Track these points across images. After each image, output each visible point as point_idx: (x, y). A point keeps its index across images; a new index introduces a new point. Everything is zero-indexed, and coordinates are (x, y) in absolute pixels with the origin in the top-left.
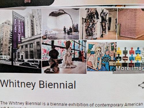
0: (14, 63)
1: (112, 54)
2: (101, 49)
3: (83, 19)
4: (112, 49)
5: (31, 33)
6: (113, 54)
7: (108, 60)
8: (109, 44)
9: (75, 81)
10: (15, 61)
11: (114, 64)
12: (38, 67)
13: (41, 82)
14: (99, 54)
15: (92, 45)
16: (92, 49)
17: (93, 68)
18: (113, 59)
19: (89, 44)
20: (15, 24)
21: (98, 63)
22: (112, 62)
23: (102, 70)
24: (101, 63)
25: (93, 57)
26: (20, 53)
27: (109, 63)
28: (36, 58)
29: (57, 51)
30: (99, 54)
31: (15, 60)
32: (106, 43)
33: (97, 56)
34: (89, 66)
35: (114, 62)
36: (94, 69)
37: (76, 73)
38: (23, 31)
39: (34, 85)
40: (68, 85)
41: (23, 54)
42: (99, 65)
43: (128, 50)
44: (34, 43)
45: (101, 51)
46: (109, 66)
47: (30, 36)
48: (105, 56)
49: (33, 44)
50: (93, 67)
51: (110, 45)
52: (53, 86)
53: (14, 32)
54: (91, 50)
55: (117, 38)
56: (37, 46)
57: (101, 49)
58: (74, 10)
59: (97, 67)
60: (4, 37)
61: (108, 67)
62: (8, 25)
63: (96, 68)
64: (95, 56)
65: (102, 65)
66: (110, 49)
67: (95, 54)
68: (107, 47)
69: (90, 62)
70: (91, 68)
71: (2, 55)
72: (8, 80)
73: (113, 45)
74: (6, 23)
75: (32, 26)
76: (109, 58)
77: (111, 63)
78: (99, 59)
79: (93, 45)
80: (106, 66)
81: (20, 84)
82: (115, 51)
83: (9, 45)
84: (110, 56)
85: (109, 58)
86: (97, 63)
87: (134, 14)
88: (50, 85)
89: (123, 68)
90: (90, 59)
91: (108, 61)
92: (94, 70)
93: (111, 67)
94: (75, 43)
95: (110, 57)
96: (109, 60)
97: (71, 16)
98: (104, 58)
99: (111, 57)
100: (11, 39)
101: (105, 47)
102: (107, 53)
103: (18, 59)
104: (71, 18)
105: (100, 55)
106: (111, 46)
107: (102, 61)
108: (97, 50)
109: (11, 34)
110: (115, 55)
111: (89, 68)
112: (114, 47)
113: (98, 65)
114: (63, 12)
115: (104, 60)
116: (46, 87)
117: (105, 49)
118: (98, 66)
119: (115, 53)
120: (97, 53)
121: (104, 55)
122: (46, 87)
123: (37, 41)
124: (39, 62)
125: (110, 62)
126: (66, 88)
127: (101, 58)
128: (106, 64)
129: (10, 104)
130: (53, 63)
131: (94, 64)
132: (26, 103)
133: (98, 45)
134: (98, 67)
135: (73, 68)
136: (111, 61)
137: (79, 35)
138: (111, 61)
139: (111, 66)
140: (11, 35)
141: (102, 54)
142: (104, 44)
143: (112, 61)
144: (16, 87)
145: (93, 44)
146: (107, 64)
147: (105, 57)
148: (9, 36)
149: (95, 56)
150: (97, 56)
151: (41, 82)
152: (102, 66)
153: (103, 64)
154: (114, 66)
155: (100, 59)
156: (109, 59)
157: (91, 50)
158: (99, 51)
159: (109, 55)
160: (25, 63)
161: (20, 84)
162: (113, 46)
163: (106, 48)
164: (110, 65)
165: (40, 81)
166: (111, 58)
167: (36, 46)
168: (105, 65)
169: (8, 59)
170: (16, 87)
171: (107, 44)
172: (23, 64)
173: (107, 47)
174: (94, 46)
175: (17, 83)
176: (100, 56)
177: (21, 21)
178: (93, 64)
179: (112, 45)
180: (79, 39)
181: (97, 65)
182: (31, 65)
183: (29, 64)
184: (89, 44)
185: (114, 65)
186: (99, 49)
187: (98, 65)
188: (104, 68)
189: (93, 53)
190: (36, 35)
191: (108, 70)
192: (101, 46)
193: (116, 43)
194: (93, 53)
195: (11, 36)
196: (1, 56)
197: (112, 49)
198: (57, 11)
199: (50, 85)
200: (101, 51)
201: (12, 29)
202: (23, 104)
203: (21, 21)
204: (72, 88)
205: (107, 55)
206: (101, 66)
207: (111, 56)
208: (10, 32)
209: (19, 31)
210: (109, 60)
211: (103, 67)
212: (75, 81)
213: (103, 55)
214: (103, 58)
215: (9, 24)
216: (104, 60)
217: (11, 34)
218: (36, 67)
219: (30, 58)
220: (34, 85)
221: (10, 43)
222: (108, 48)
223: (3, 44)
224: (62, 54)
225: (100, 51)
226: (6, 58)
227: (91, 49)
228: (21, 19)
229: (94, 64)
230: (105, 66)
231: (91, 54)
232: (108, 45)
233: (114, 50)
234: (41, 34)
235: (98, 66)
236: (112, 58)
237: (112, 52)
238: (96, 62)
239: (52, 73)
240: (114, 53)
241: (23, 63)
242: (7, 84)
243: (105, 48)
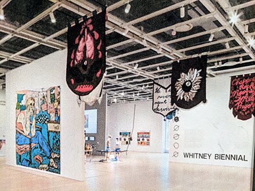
2: (34, 100)
4: (53, 101)
7: (46, 120)
8: (47, 91)
16: (22, 101)
19: (18, 95)
21: (31, 124)
22: (52, 124)
24: (36, 125)
32: (41, 91)
34: (18, 130)
35: (56, 125)
36: (25, 135)
42: (32, 129)
46: (48, 133)
48: (41, 113)
51: (49, 92)
54: (20, 104)
57: (34, 100)
59: (29, 132)
63: (28, 135)
66: (49, 101)
67: (26, 111)
68: (44, 97)
69: (19, 123)
76: (46, 117)
77: (51, 127)
79: (24, 95)
82: (57, 104)
84: (49, 113)
85: (46, 117)
86: (29, 125)
90: (20, 119)
93: (50, 133)
95: (49, 114)
96: (48, 120)
98: (39, 117)
99: (51, 114)
101: (41, 97)
105: (34, 112)
107: (37, 122)
108: (29, 104)
110: (57, 112)
111: (20, 133)
112: (55, 97)
113: (31, 128)
115: (39, 120)
119: (58, 108)
120: (28, 108)
121: (40, 112)
125: (48, 124)
127: (35, 116)
131: (26, 127)
133: (29, 95)
134: (30, 132)
136: (51, 122)
139: (52, 131)
142: (39, 92)
143: (53, 122)
145: (24, 93)
150: (27, 113)
153: (38, 128)
155: (34, 119)
156: (47, 119)
157: (20, 104)
158: (31, 104)
159: (47, 111)
162: (54, 94)
163: (43, 99)
164: (49, 129)
166: (50, 116)
173: (44, 97)
174: (24, 97)
176: (32, 113)
178: (24, 126)
179: (52, 93)
181: (29, 129)
184: (18, 95)
186: (32, 102)
187: (31, 128)
192: (34, 96)
193: (59, 87)
197: (51, 99)
200: (34, 104)
205: (43, 111)
206: (35, 131)
207: (51, 112)
210: (48, 120)
211: (39, 132)
213: (38, 112)
214: (38, 116)
216: (39, 120)
222: (46, 98)
230: (41, 131)
232: (45, 93)
233: (56, 101)
236: (53, 118)
238: (28, 123)
240: (55, 107)
243: (41, 99)
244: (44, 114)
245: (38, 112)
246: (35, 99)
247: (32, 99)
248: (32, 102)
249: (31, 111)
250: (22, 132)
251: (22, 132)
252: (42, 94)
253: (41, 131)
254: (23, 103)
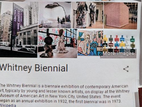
0: (13, 48)
1: (99, 41)
2: (89, 36)
3: (74, 10)
4: (100, 36)
5: (29, 22)
6: (100, 41)
7: (96, 46)
8: (96, 32)
9: (67, 65)
10: (13, 47)
11: (101, 49)
12: (34, 52)
13: (36, 65)
14: (87, 40)
15: (82, 33)
16: (82, 36)
17: (83, 53)
18: (100, 45)
19: (79, 32)
21: (87, 48)
22: (99, 48)
23: (90, 55)
24: (90, 48)
25: (83, 44)
26: (19, 40)
27: (96, 49)
28: (33, 44)
29: (52, 38)
30: (87, 40)
31: (14, 46)
33: (86, 43)
34: (79, 51)
35: (101, 48)
37: (68, 58)
38: (22, 20)
39: (30, 69)
40: (61, 69)
41: (21, 40)
42: (88, 50)
43: (114, 37)
44: (32, 31)
45: (90, 38)
46: (97, 52)
47: (28, 25)
48: (93, 42)
49: (31, 32)
50: (82, 52)
51: (98, 33)
52: (47, 69)
53: (14, 21)
54: (81, 37)
55: (103, 27)
56: (34, 33)
57: (89, 36)
58: (67, 3)
59: (86, 52)
60: (4, 25)
61: (96, 52)
62: (9, 15)
63: (86, 53)
64: (84, 43)
65: (91, 50)
66: (97, 36)
67: (84, 41)
68: (95, 35)
69: (80, 47)
70: (82, 53)
71: (2, 41)
72: (6, 64)
73: (100, 33)
74: (7, 13)
75: (30, 16)
77: (99, 49)
78: (88, 45)
79: (83, 33)
80: (94, 51)
81: (17, 67)
83: (9, 33)
86: (86, 49)
87: (117, 7)
88: (45, 68)
89: (109, 54)
90: (80, 45)
91: (96, 47)
92: (84, 54)
93: (98, 52)
94: (67, 31)
95: (98, 43)
96: (97, 46)
97: (64, 8)
98: (92, 44)
99: (99, 43)
100: (11, 27)
101: (93, 34)
102: (95, 40)
103: (17, 45)
104: (64, 10)
105: (89, 42)
106: (99, 34)
107: (90, 47)
109: (11, 23)
111: (80, 53)
112: (100, 35)
113: (87, 50)
114: (58, 5)
115: (92, 46)
116: (41, 71)
117: (93, 37)
118: (87, 51)
119: (102, 40)
120: (86, 40)
121: (92, 42)
122: (41, 71)
123: (35, 29)
124: (35, 48)
125: (97, 48)
126: (59, 71)
127: (90, 44)
128: (94, 49)
129: (7, 86)
130: (48, 48)
131: (84, 49)
132: (23, 86)
133: (87, 33)
134: (87, 52)
135: (65, 53)
136: (98, 47)
137: (70, 24)
138: (98, 47)
140: (11, 24)
141: (90, 41)
142: (92, 32)
143: (100, 47)
144: (13, 70)
145: (83, 32)
146: (95, 50)
147: (93, 44)
148: (9, 25)
149: (84, 43)
150: (86, 42)
151: (36, 65)
152: (90, 51)
153: (91, 50)
154: (101, 51)
156: (97, 45)
157: (81, 37)
158: (87, 38)
159: (96, 41)
160: (23, 48)
161: (17, 67)
162: (100, 34)
163: (94, 36)
164: (97, 50)
165: (36, 65)
166: (98, 44)
167: (33, 34)
168: (93, 50)
169: (8, 45)
170: (13, 70)
171: (94, 32)
172: (21, 49)
173: (95, 35)
174: (83, 34)
175: (15, 67)
176: (88, 42)
177: (20, 12)
178: (83, 49)
179: (99, 33)
180: (70, 28)
181: (86, 50)
182: (28, 50)
183: (26, 49)
184: (79, 32)
185: (101, 50)
186: (88, 37)
187: (87, 50)
188: (93, 53)
189: (82, 40)
190: (33, 24)
191: (96, 55)
192: (89, 34)
193: (103, 31)
194: (82, 40)
195: (11, 25)
196: (1, 42)
197: (99, 36)
198: (52, 4)
199: (45, 68)
200: (89, 38)
201: (12, 19)
202: (20, 86)
203: (20, 12)
204: (64, 71)
205: (95, 41)
206: (89, 51)
208: (10, 21)
209: (19, 20)
210: (97, 46)
211: (92, 52)
212: (67, 65)
213: (91, 42)
214: (91, 44)
215: (9, 14)
216: (92, 46)
217: (11, 23)
218: (33, 52)
219: (28, 44)
220: (30, 69)
221: (10, 31)
222: (96, 35)
223: (3, 31)
224: (56, 41)
225: (88, 38)
226: (5, 44)
227: (81, 36)
228: (21, 10)
229: (84, 49)
230: (93, 51)
231: (81, 41)
232: (96, 33)
233: (101, 37)
234: (37, 23)
235: (87, 51)
236: (100, 45)
237: (99, 39)
238: (86, 47)
239: (46, 57)
240: (101, 40)
241: (21, 48)
242: (6, 68)
243: (93, 36)
244: (95, 43)
245: (91, 42)
246: (90, 35)
247: (88, 35)
248: (88, 37)
249: (87, 41)
250: (82, 53)
251: (82, 53)
252: (94, 33)
253: (93, 51)
254: (83, 37)
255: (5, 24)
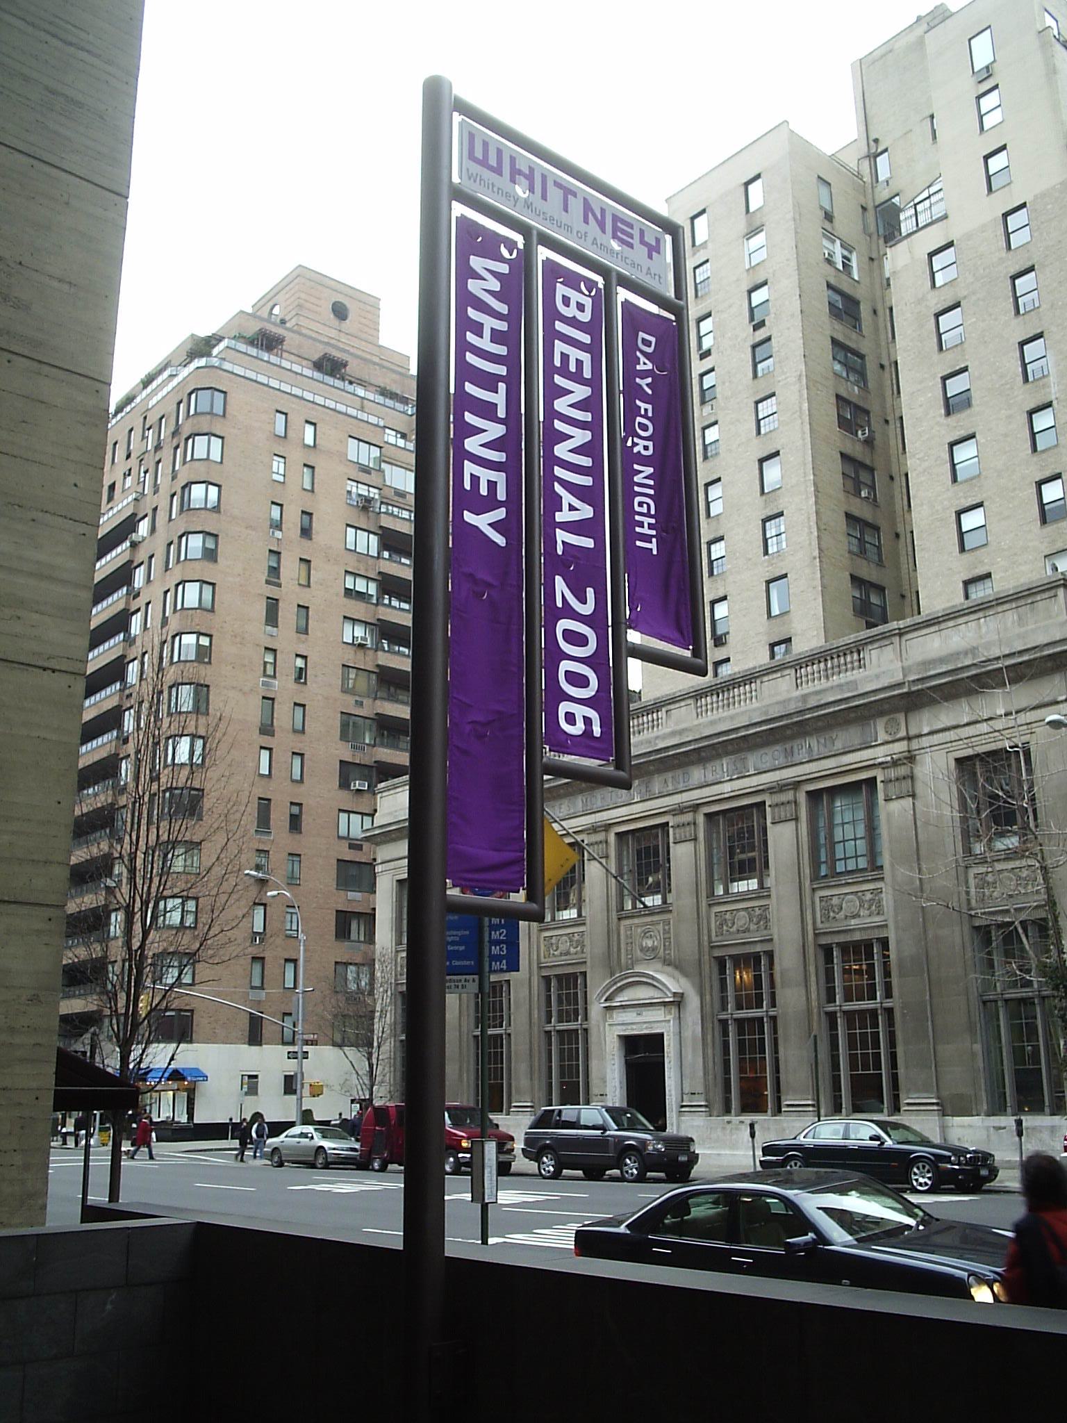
0: (457, 1194)
10: (472, 1169)
20: (467, 373)
26: (597, 988)
28: (950, 1107)
31: (486, 1130)
38: (644, 504)
44: (908, 787)
47: (808, 638)
49: (893, 812)
53: (442, 542)
56: (968, 835)
60: (224, 648)
74: (268, 342)
83: (356, 826)
100: (387, 679)
103: (544, 1120)
109: (389, 586)
123: (982, 739)
124: (1010, 1179)
140: (400, 613)
160: (729, 1198)
167: (951, 842)
169: (348, 1128)
172: (651, 1220)
177: (604, 301)
182: (840, 1239)
183: (798, 1221)
190: (952, 615)
195: (387, 632)
201: (405, 481)
203: (604, 301)
208: (368, 543)
209: (573, 510)
215: (330, 366)
217: (389, 586)
218: (958, 1289)
221: (386, 772)
223: (214, 785)
226: (275, 1107)
228: (612, 252)
255: (258, 630)
